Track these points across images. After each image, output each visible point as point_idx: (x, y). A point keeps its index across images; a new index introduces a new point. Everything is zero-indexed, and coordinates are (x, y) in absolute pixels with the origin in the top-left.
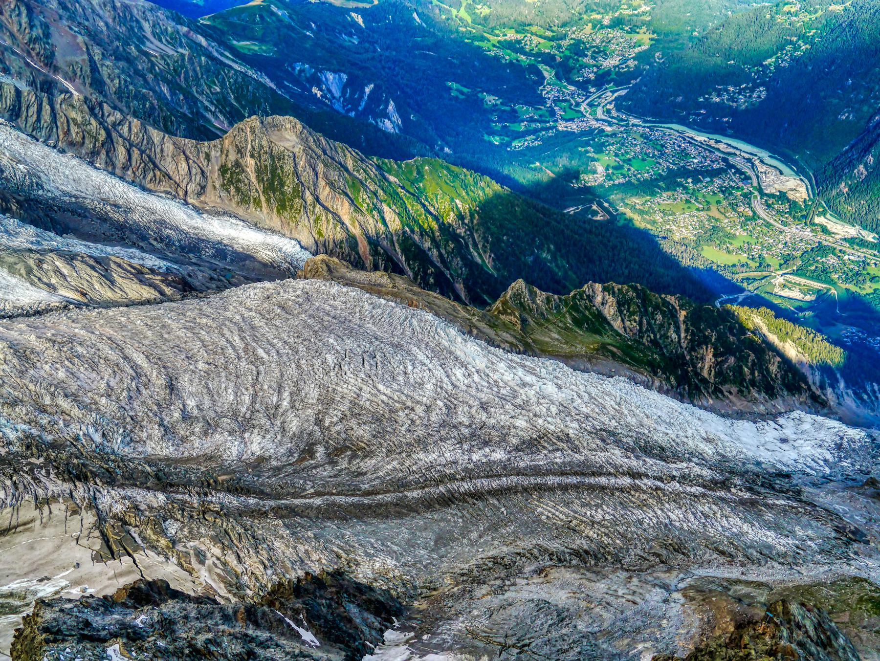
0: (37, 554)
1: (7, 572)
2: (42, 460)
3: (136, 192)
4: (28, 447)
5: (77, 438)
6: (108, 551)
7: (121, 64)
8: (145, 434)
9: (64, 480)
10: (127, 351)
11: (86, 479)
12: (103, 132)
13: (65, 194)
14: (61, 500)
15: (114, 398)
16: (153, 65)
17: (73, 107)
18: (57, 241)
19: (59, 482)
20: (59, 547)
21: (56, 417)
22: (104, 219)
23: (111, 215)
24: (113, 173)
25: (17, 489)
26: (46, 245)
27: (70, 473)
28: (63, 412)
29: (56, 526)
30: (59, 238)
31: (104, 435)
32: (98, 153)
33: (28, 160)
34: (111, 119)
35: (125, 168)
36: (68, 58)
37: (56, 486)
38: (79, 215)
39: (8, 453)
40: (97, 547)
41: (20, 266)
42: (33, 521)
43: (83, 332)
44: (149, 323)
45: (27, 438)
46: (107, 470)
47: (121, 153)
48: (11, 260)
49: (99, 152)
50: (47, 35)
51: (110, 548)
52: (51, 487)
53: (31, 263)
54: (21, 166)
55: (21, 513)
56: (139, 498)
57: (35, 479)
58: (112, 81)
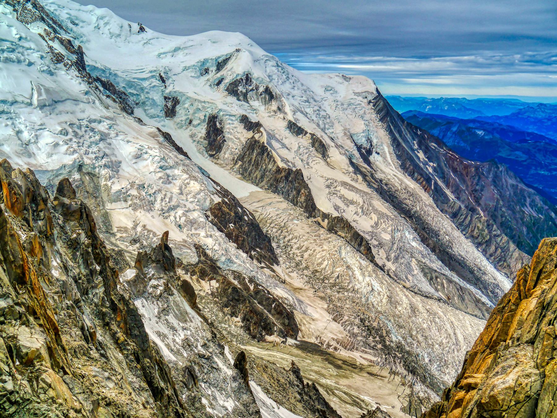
0: (380, 392)
1: (366, 391)
2: (401, 355)
3: (491, 267)
4: (398, 347)
5: (418, 355)
6: (408, 410)
7: (510, 212)
8: (447, 371)
9: (405, 369)
10: (456, 331)
11: (414, 374)
12: (488, 237)
13: (460, 255)
14: (400, 376)
15: (442, 348)
16: (524, 217)
17: (480, 222)
18: (448, 272)
19: (403, 369)
20: (390, 395)
21: (414, 342)
22: (472, 272)
23: (475, 272)
24: (485, 255)
25: (386, 361)
26: (443, 271)
27: (409, 367)
28: (418, 341)
29: (393, 385)
30: (449, 271)
31: (430, 361)
32: (482, 245)
33: (451, 236)
34: (495, 233)
35: (491, 255)
36: (488, 202)
37: (401, 369)
38: (462, 266)
39: (389, 345)
40: (405, 405)
41: (429, 275)
42: (385, 377)
43: (442, 314)
44: (472, 325)
45: (399, 343)
46: (424, 376)
47: (493, 248)
48: (427, 271)
49: (482, 244)
50: (482, 190)
51: (410, 409)
52: (399, 368)
53: (434, 275)
54: (447, 237)
55: (383, 371)
56: (432, 396)
57: (394, 361)
58: (502, 217)
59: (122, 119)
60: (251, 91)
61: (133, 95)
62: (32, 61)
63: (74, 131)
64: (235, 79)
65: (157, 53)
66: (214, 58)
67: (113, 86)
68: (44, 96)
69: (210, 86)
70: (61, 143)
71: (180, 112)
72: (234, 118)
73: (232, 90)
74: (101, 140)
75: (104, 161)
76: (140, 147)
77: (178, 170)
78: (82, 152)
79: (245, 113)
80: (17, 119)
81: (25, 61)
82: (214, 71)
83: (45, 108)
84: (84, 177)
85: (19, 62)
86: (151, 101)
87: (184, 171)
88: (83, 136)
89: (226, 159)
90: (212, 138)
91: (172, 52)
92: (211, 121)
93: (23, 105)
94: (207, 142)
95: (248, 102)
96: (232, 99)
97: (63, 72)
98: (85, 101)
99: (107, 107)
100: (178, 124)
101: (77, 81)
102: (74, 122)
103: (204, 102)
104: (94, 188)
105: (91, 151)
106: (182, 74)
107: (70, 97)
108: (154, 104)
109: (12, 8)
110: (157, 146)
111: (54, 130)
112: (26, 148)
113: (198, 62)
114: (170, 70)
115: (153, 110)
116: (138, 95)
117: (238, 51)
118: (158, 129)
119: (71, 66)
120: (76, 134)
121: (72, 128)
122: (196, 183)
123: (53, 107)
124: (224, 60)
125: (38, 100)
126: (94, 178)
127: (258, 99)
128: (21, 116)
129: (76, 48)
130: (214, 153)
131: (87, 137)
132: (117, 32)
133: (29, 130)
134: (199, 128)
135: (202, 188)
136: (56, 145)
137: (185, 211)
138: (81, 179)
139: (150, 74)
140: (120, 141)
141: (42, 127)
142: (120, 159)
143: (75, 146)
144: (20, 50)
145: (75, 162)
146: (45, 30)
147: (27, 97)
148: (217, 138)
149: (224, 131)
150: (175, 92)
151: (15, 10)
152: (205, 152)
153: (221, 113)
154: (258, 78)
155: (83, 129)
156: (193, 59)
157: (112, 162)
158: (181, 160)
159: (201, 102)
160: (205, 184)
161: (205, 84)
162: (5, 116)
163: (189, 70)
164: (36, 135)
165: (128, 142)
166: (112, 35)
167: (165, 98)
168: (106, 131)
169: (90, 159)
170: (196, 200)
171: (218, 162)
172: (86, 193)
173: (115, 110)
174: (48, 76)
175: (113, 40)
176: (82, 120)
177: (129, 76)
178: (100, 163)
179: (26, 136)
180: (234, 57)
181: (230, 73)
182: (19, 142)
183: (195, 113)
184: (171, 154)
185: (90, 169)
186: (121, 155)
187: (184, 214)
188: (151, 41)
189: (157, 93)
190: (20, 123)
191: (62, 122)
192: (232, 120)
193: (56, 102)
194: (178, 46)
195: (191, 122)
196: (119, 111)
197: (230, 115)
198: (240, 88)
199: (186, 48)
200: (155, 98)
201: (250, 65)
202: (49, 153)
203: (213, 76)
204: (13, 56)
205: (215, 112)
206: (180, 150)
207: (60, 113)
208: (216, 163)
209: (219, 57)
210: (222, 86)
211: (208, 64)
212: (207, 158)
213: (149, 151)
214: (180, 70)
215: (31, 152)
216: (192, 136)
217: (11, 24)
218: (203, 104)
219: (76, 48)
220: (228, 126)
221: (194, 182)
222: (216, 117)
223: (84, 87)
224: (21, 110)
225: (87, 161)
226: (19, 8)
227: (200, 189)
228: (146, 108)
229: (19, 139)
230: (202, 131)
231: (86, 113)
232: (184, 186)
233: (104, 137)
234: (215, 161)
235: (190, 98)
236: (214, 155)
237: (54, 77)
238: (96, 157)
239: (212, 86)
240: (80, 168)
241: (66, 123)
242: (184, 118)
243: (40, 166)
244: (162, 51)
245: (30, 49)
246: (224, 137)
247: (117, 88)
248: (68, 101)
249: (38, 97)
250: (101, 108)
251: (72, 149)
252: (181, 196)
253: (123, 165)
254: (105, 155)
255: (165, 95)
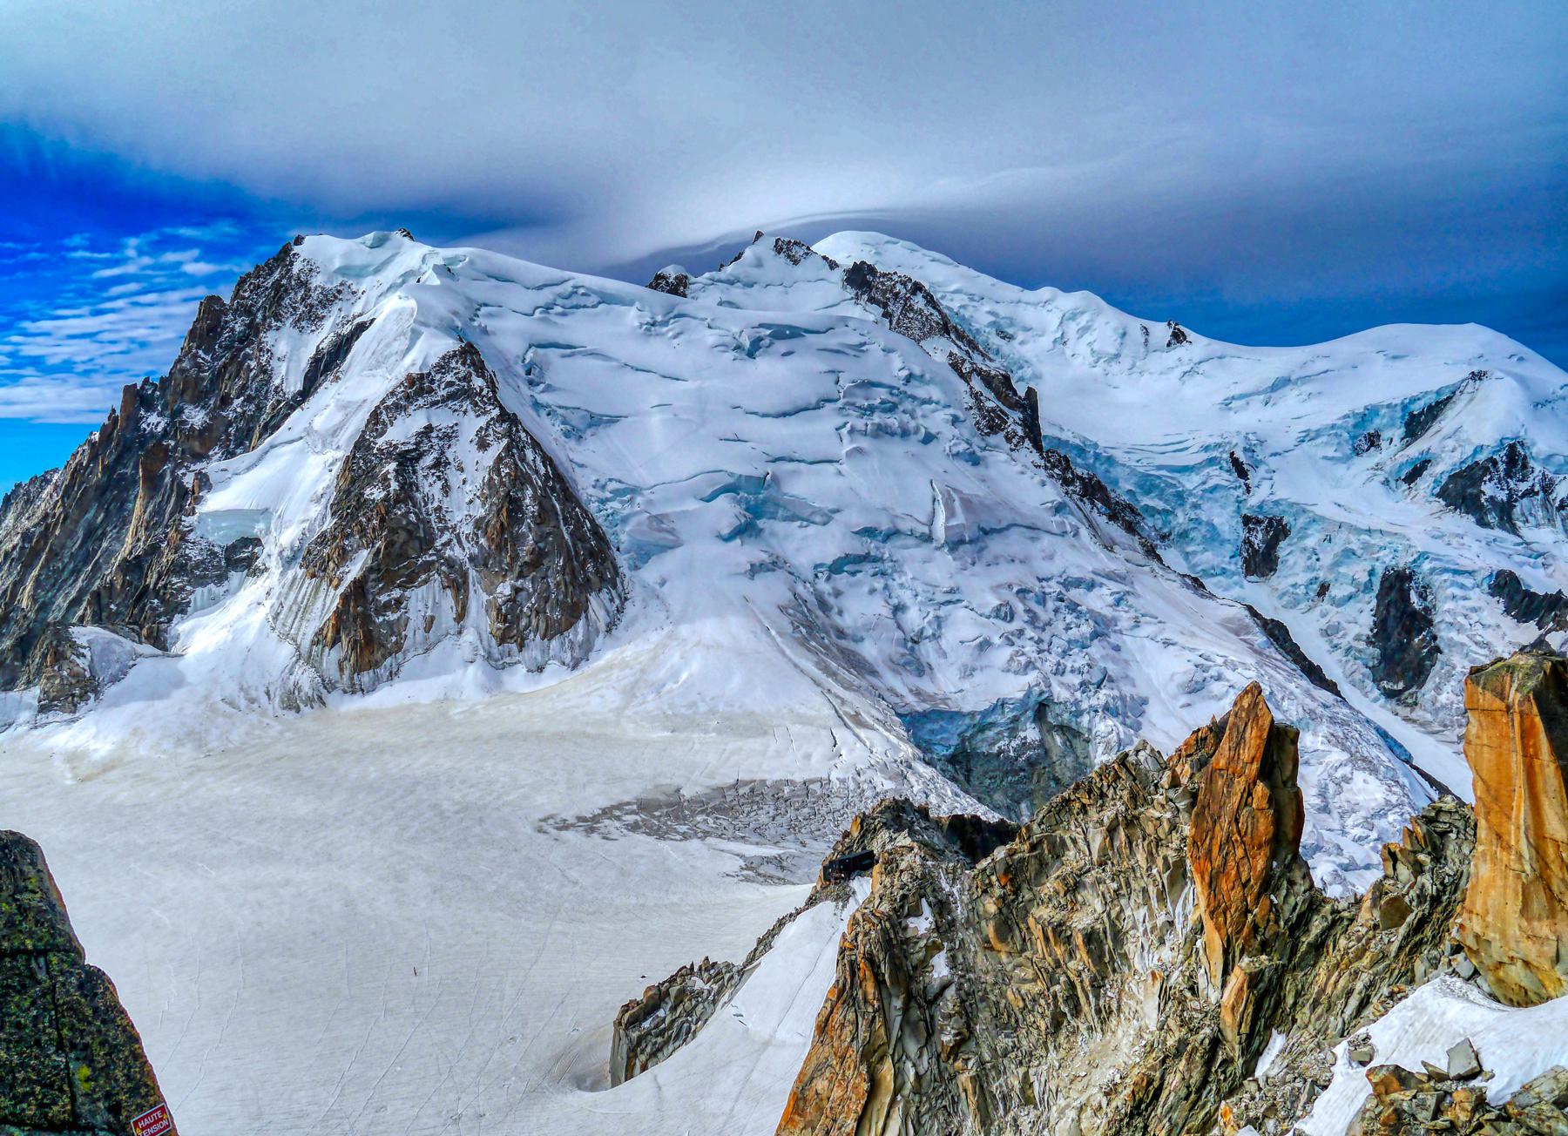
59: (1149, 580)
60: (1524, 495)
61: (1153, 511)
62: (933, 431)
63: (1029, 608)
64: (1470, 463)
65: (1220, 400)
66: (1398, 401)
67: (1103, 489)
68: (960, 519)
69: (1386, 482)
70: (996, 640)
71: (1291, 559)
72: (1468, 582)
73: (1461, 492)
74: (1096, 635)
75: (1103, 696)
76: (1201, 661)
77: (1315, 734)
78: (1049, 666)
79: (1506, 565)
80: (896, 576)
81: (917, 430)
82: (1396, 441)
83: (962, 548)
84: (1049, 738)
85: (905, 433)
86: (1203, 529)
87: (1333, 740)
88: (1049, 624)
89: (1443, 707)
90: (1395, 637)
91: (1264, 392)
92: (1391, 587)
93: (911, 541)
94: (1377, 651)
95: (1514, 530)
96: (1462, 523)
97: (1003, 457)
98: (1056, 530)
99: (1109, 546)
100: (1284, 594)
101: (1037, 479)
102: (1029, 586)
103: (1369, 531)
104: (1075, 769)
105: (1069, 665)
106: (1298, 451)
107: (1019, 521)
108: (1213, 537)
109: (881, 311)
110: (1251, 660)
111: (980, 606)
112: (912, 649)
113: (1347, 416)
114: (1262, 442)
115: (1208, 555)
116: (1167, 512)
117: (1477, 376)
118: (1250, 609)
119: (1022, 439)
120: (1033, 619)
121: (1023, 600)
122: (1371, 779)
123: (980, 544)
124: (1430, 407)
125: (947, 529)
126: (1077, 743)
127: (1551, 521)
128: (906, 568)
129: (1022, 393)
130: (1401, 686)
131: (1060, 625)
132: (1113, 351)
133: (921, 603)
134: (1351, 609)
135: (1394, 799)
136: (985, 645)
137: (1340, 865)
138: (1042, 741)
139: (1205, 456)
140: (1147, 642)
141: (953, 597)
142: (1142, 691)
143: (1030, 648)
144: (908, 405)
145: (1028, 695)
146: (951, 354)
147: (924, 520)
148: (1409, 643)
149: (1437, 619)
150: (1276, 503)
151: (887, 315)
152: (1369, 684)
153: (1426, 566)
154: (1551, 456)
155: (1051, 605)
156: (1333, 407)
157: (1122, 698)
158: (1325, 706)
159: (1359, 531)
160: (1403, 787)
161: (1370, 479)
162: (869, 568)
163: (1319, 441)
164: (937, 617)
165: (1167, 643)
166: (1097, 357)
167: (1247, 520)
168: (1108, 612)
169: (1068, 687)
170: (1374, 835)
171: (1413, 716)
172: (1052, 784)
173: (1129, 554)
174: (968, 466)
175: (1098, 370)
176: (1047, 580)
177: (1145, 462)
178: (1094, 702)
179: (914, 618)
180: (1466, 397)
181: (1451, 443)
182: (899, 634)
183: (1337, 564)
184: (1292, 686)
185: (1066, 716)
186: (1149, 680)
187: (1336, 874)
188: (1205, 366)
189: (1222, 507)
190: (902, 585)
191: (999, 586)
192: (1462, 586)
193: (986, 533)
194: (1285, 374)
195: (1324, 589)
196: (1139, 557)
197: (1456, 572)
198: (1489, 489)
199: (1305, 379)
200: (1216, 521)
201: (1522, 417)
202: (965, 666)
203: (1394, 453)
204: (893, 421)
205: (1404, 561)
206: (1314, 673)
207: (995, 562)
208: (1406, 719)
209: (1414, 400)
210: (1425, 484)
211: (1377, 422)
212: (1376, 700)
213: (1228, 674)
214: (1290, 440)
215: (924, 660)
216: (1326, 633)
217: (890, 346)
218: (1365, 537)
219: (1022, 393)
220: (1449, 605)
221: (1366, 775)
222: (1410, 578)
223: (1053, 493)
224: (906, 552)
225: (1060, 693)
226: (895, 308)
227: (1388, 802)
228: (1190, 549)
229: (899, 627)
230: (1361, 618)
231: (1057, 559)
232: (1332, 788)
233: (1102, 629)
234: (1405, 711)
235: (1323, 518)
236: (1401, 692)
237: (981, 470)
238: (1082, 684)
239: (1393, 484)
240: (1041, 710)
241: (1010, 586)
242: (1303, 578)
243: (945, 700)
244: (1236, 391)
245: (929, 401)
246: (1435, 638)
247: (1112, 495)
248: (1015, 530)
249: (947, 519)
250: (1095, 548)
251: (1023, 659)
252: (1324, 816)
253: (1153, 711)
254: (1106, 679)
255: (1244, 512)
